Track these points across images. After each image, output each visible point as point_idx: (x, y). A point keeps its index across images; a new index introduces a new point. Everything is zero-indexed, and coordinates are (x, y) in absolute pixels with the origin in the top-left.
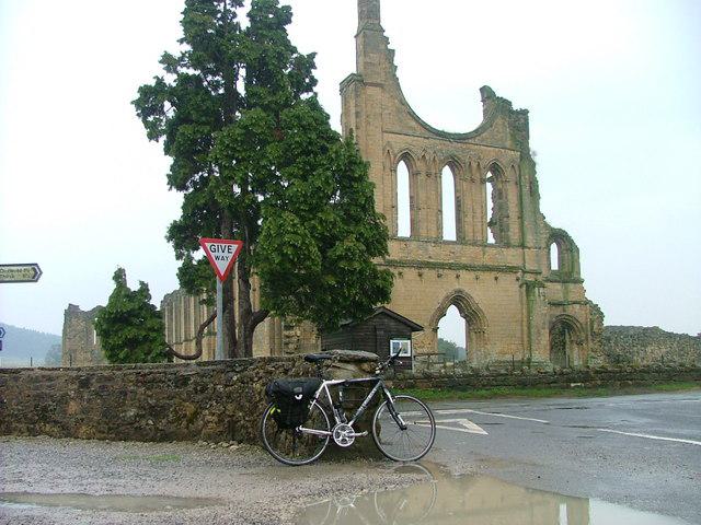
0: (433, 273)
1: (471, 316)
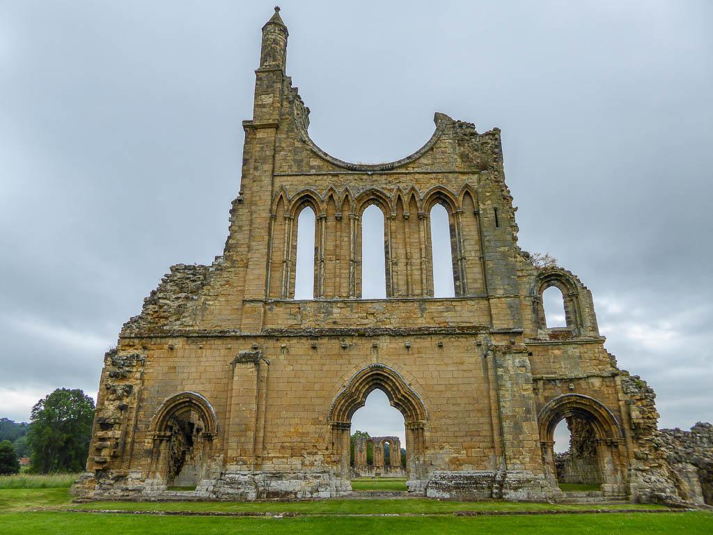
0: (335, 344)
1: (404, 403)
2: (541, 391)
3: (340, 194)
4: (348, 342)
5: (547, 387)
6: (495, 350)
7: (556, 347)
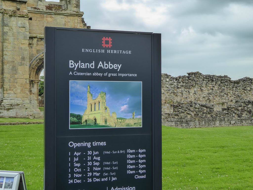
2: (35, 45)
5: (39, 43)
7: (50, 15)
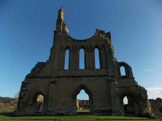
2: (120, 90)
3: (75, 46)
4: (76, 78)
6: (109, 80)
